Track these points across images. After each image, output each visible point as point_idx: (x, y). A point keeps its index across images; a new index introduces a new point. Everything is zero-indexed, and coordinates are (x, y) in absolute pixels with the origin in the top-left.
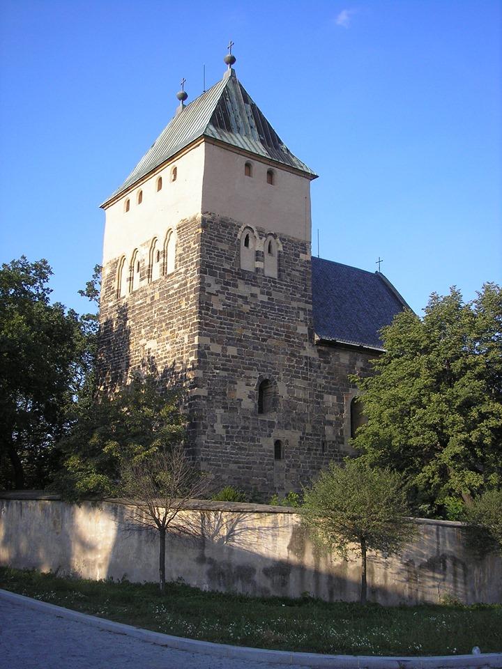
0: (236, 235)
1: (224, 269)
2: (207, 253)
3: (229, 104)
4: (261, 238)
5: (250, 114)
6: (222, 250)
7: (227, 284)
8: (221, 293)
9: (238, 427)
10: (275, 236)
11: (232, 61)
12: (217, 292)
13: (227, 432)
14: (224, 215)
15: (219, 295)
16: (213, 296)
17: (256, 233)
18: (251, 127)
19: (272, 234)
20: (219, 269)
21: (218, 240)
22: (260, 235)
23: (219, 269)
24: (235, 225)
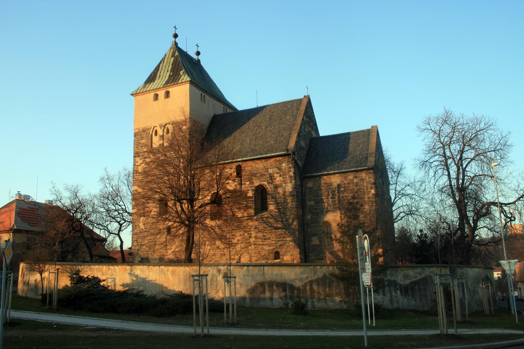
0: (149, 133)
1: (144, 152)
2: (136, 148)
3: (161, 65)
4: (161, 129)
5: (171, 63)
6: (143, 143)
7: (146, 158)
8: (142, 163)
9: (149, 223)
10: (169, 123)
11: (176, 36)
12: (141, 164)
13: (145, 226)
14: (143, 127)
15: (142, 164)
16: (139, 166)
17: (159, 127)
18: (168, 71)
19: (167, 124)
20: (142, 152)
21: (141, 140)
22: (160, 127)
23: (142, 152)
24: (149, 129)
